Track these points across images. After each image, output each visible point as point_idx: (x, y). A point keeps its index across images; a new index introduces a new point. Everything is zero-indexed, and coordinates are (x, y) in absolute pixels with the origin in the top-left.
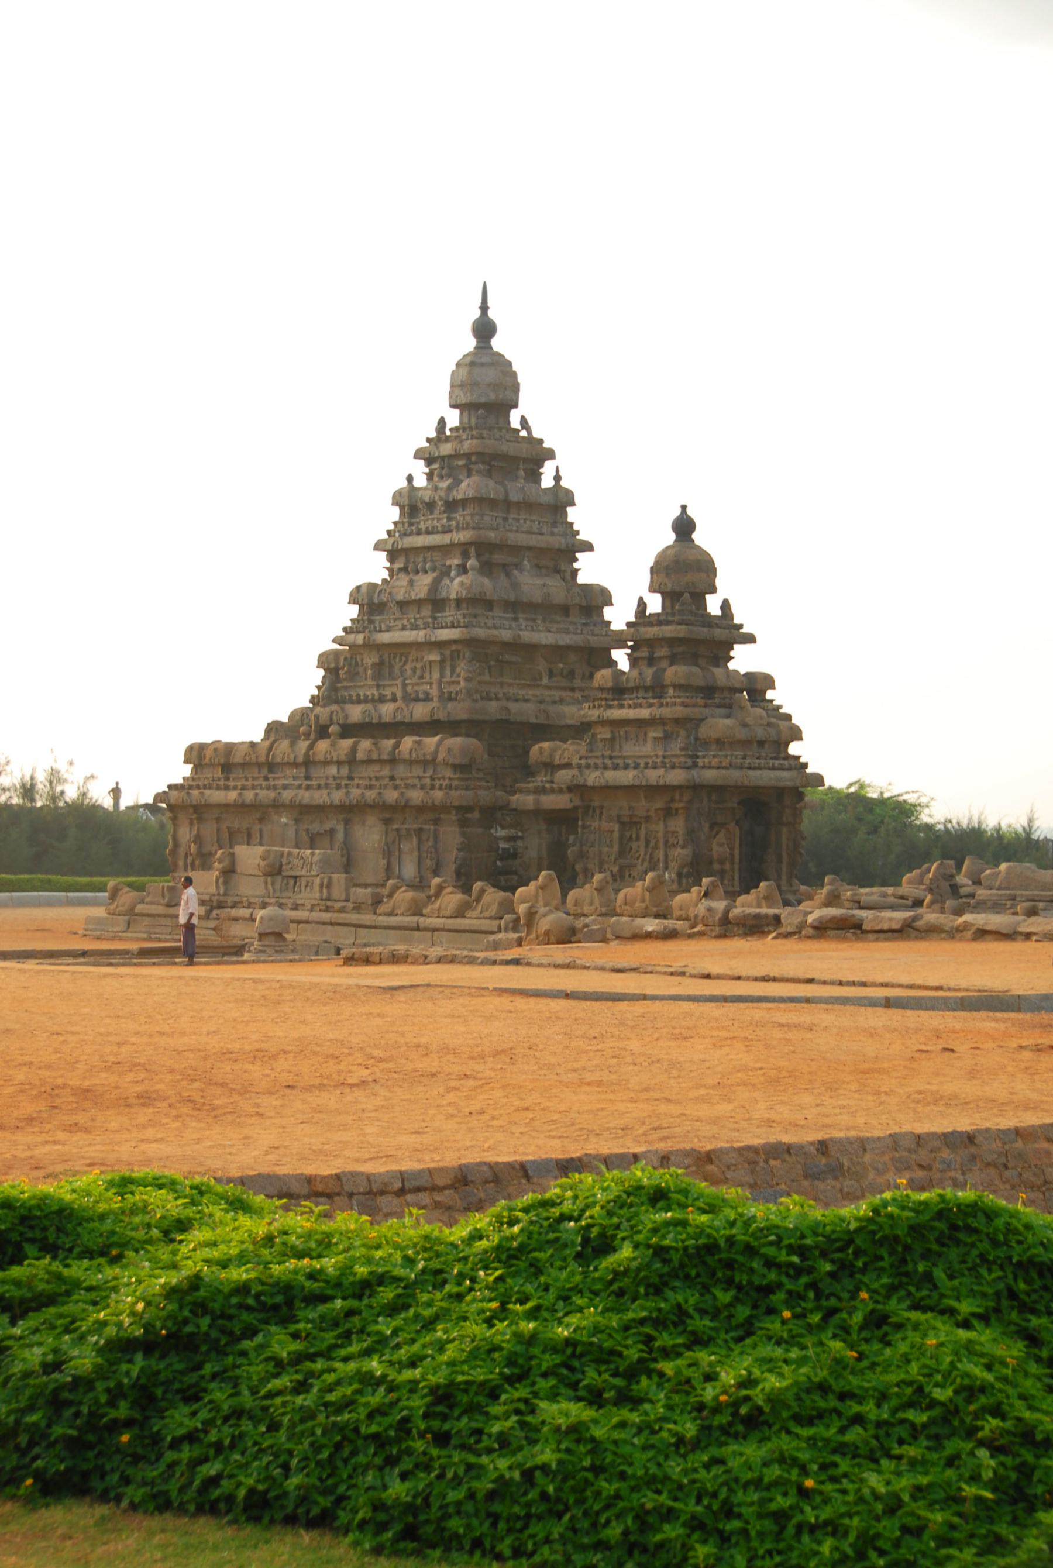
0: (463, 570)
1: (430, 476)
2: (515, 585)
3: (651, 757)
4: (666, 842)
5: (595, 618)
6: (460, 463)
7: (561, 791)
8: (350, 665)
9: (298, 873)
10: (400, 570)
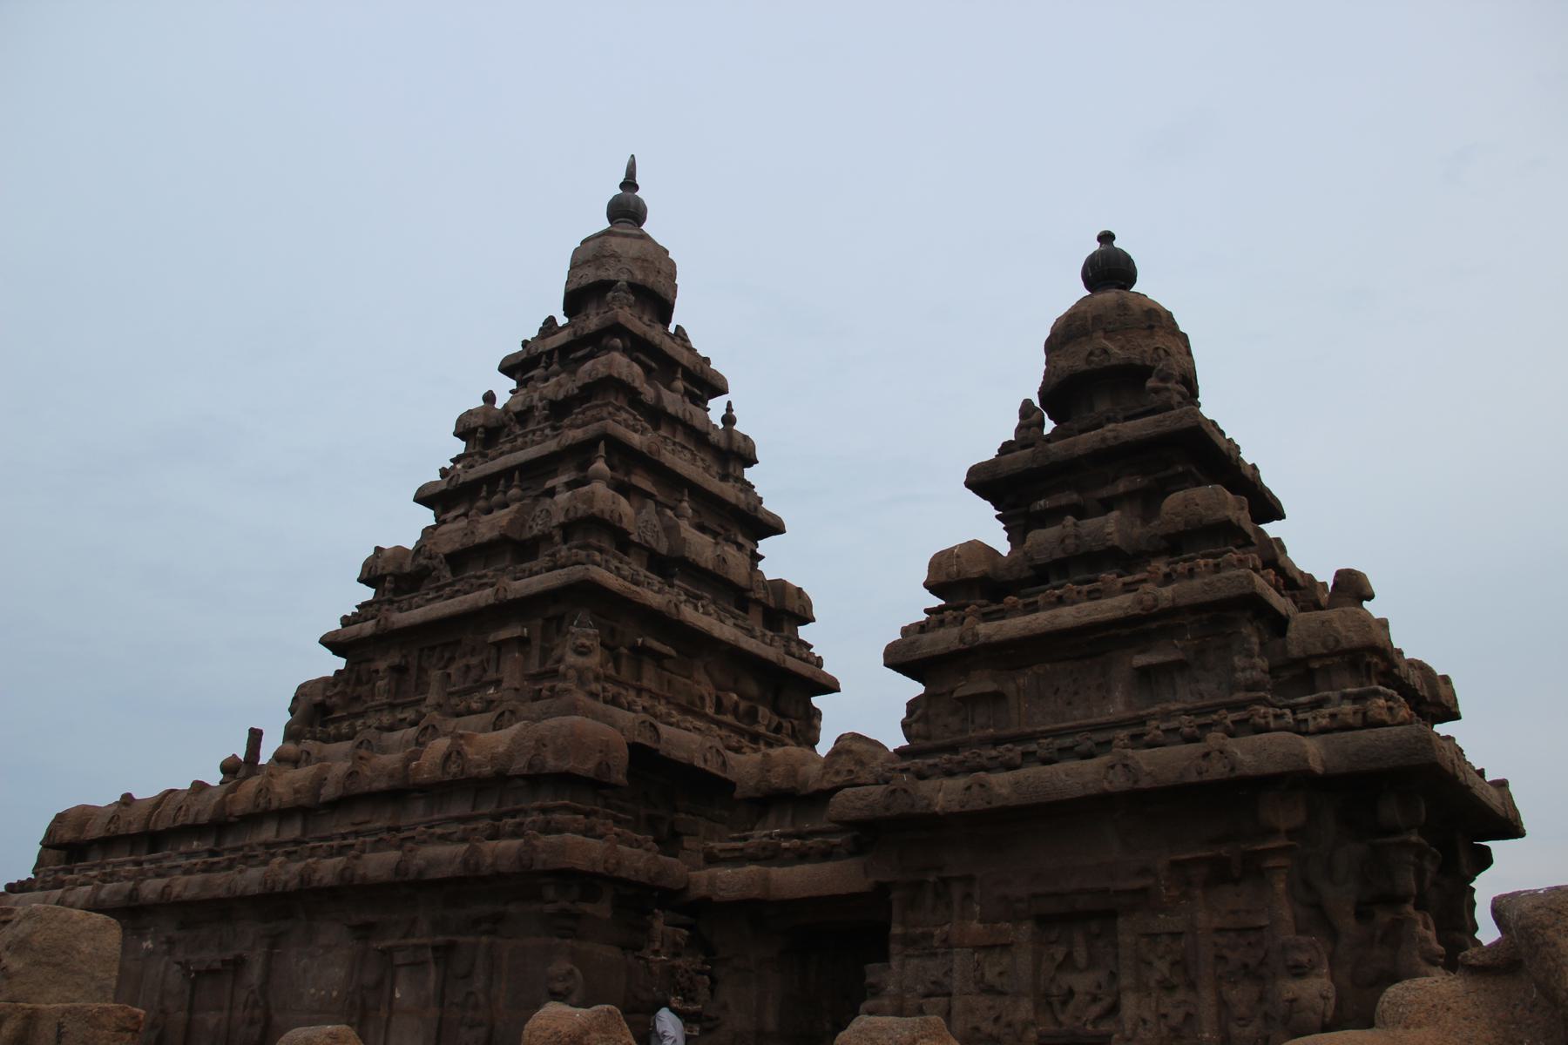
2: (671, 530)
3: (1142, 721)
4: (1221, 958)
5: (786, 633)
6: (579, 354)
7: (826, 855)
8: (347, 682)
10: (457, 517)
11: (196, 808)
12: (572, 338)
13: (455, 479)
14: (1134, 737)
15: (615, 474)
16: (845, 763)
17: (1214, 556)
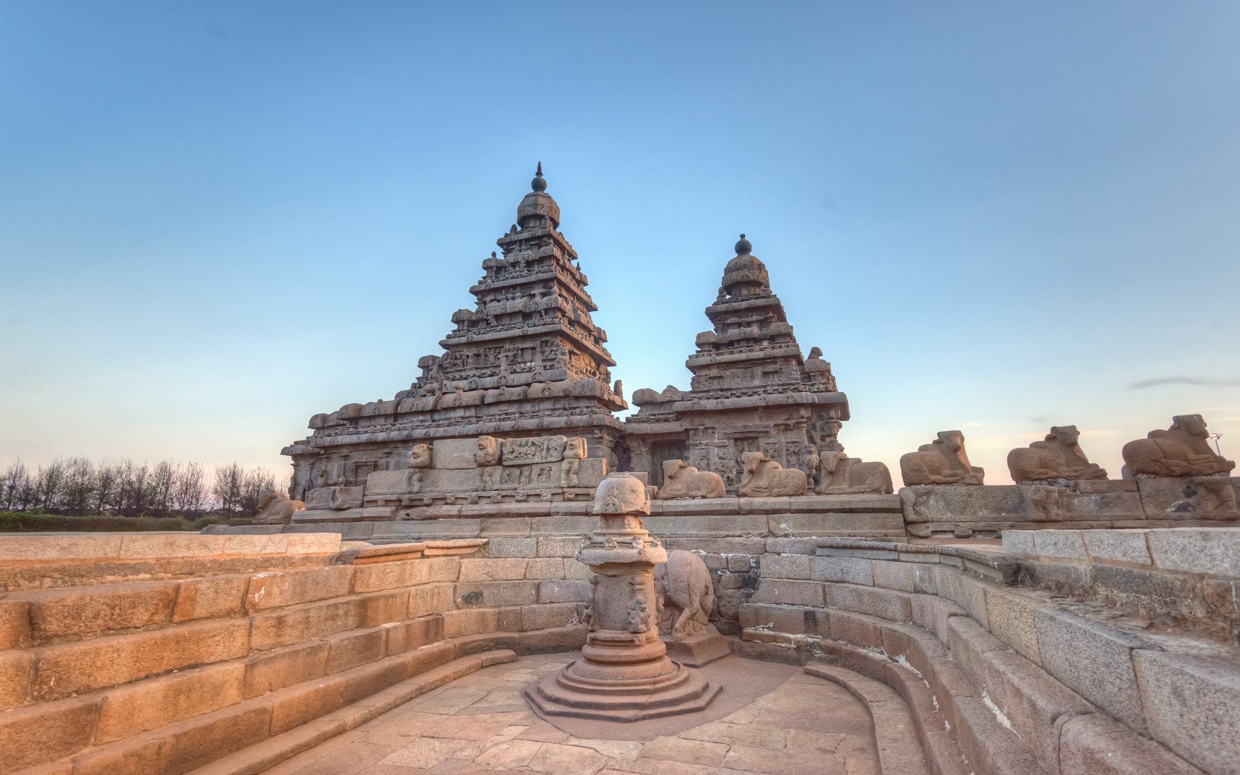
0: (544, 295)
1: (507, 252)
2: (575, 311)
6: (533, 243)
7: (666, 420)
8: (451, 358)
9: (527, 462)
11: (422, 405)
12: (530, 236)
13: (488, 287)
14: (764, 391)
16: (668, 394)
17: (786, 343)
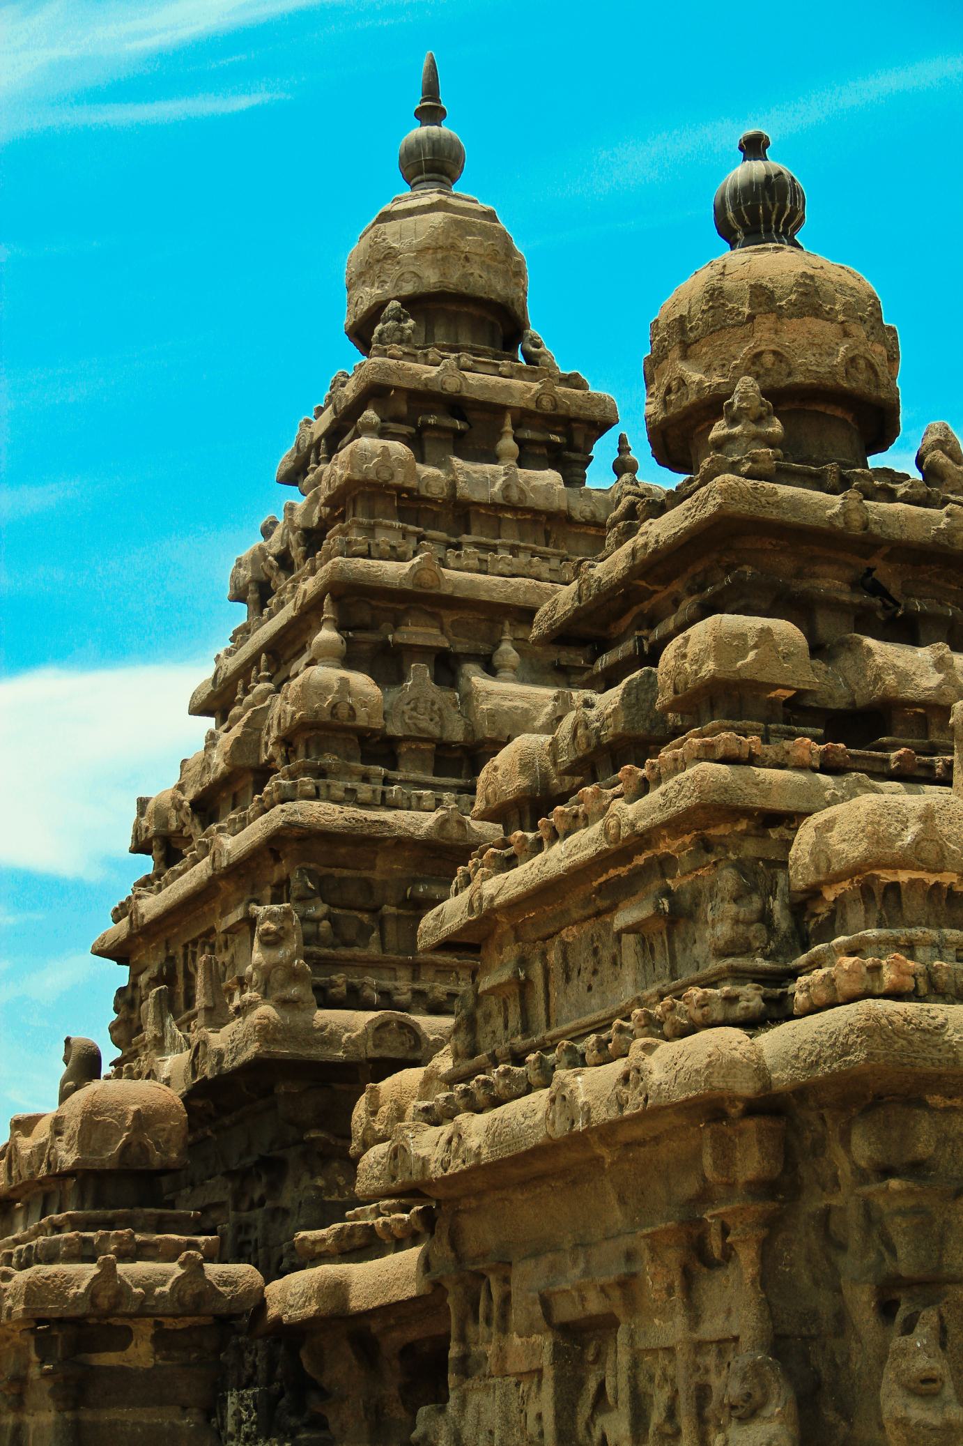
7: (414, 1239)
15: (361, 636)
